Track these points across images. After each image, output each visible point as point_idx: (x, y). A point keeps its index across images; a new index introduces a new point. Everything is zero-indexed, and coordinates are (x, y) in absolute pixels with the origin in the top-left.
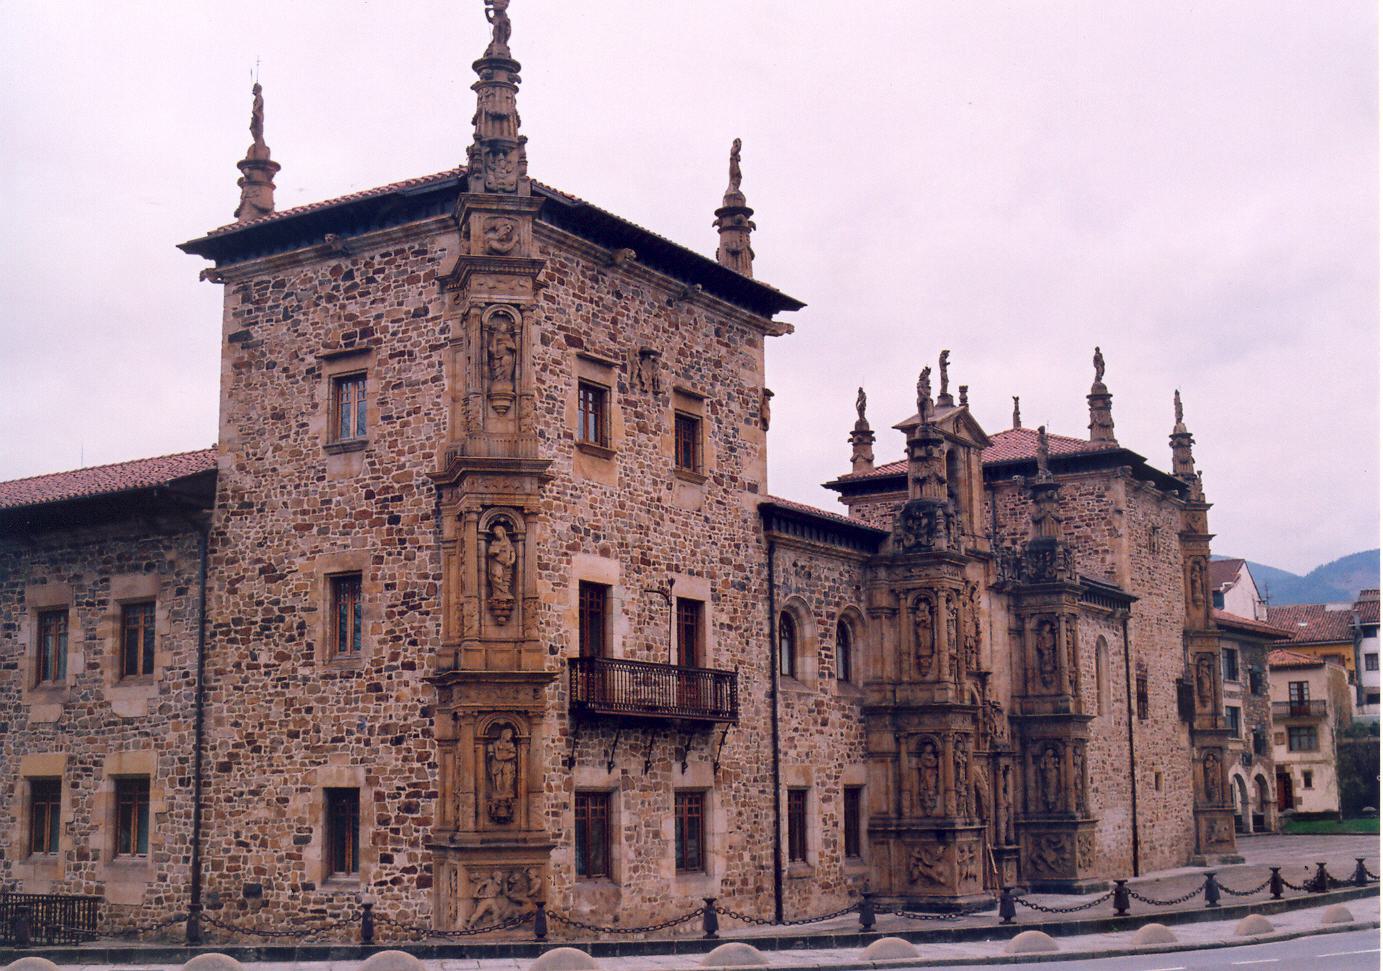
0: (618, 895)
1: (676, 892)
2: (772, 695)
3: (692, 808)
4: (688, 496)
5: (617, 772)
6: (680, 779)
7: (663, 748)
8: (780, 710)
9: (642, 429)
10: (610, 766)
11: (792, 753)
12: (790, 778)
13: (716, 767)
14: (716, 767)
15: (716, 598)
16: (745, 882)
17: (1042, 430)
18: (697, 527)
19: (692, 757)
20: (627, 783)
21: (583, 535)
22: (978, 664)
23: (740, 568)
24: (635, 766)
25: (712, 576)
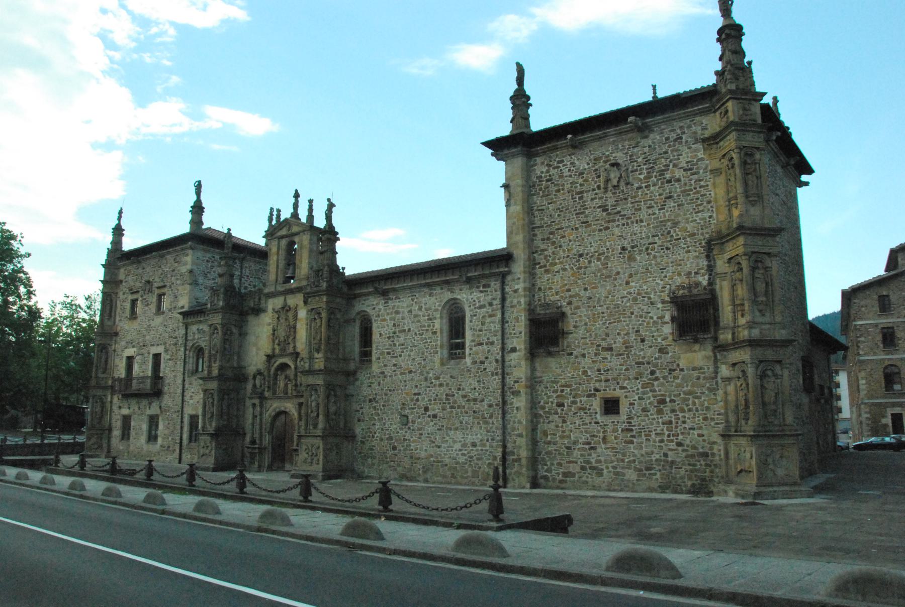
0: (129, 445)
1: (145, 447)
2: (184, 380)
3: (153, 421)
4: (159, 320)
5: (131, 410)
6: (149, 412)
7: (145, 402)
8: (186, 386)
9: (147, 305)
10: (129, 408)
11: (191, 401)
12: (189, 411)
13: (160, 407)
14: (160, 407)
15: (166, 350)
16: (169, 447)
17: (498, 146)
18: (161, 329)
19: (154, 404)
20: (134, 413)
21: (130, 343)
22: (295, 347)
23: (176, 338)
24: (136, 409)
25: (165, 344)
